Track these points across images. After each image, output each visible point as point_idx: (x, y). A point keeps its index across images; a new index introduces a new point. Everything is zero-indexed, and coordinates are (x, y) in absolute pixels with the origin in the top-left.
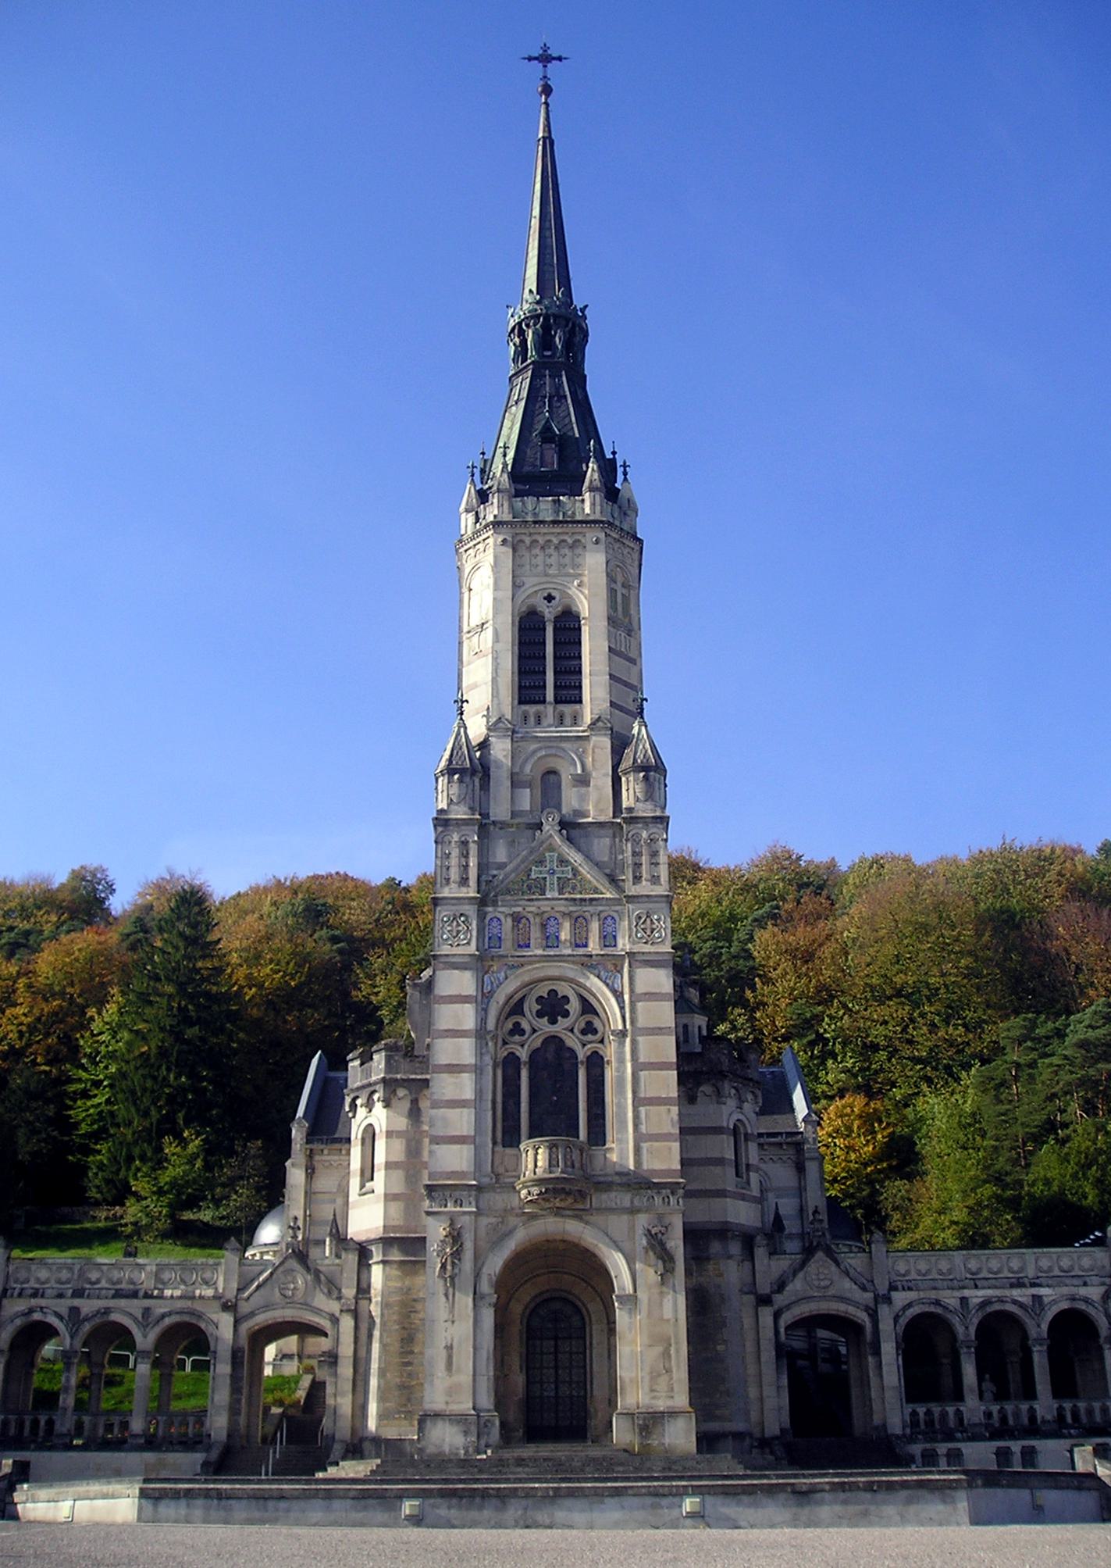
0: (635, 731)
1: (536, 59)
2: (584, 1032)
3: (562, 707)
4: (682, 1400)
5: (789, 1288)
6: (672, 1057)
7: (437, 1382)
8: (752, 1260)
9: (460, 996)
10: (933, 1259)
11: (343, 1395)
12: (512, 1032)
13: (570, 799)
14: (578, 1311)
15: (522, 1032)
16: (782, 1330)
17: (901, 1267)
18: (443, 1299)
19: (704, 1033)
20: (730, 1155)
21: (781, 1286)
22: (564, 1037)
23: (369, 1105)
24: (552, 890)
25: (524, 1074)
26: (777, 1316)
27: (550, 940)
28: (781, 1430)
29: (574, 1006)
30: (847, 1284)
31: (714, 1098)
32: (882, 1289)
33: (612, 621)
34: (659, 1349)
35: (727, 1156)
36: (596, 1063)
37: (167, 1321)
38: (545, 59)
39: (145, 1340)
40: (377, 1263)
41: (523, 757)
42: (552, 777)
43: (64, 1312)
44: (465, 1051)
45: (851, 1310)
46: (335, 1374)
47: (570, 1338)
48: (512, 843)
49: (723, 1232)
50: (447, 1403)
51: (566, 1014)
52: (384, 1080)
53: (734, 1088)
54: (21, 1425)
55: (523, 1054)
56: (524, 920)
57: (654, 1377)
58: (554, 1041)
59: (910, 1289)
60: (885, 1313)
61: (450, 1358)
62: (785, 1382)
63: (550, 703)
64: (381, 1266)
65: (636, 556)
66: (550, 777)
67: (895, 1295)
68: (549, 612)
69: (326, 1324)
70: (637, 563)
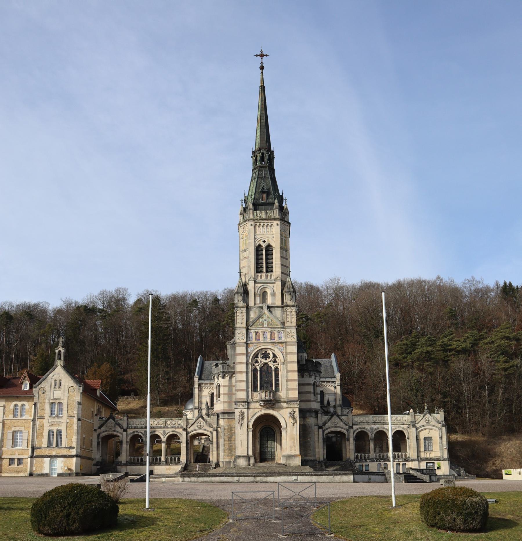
0: (288, 279)
1: (259, 55)
2: (274, 362)
3: (268, 273)
4: (298, 452)
6: (296, 369)
9: (242, 353)
12: (255, 363)
13: (270, 301)
14: (273, 430)
15: (258, 362)
17: (356, 419)
18: (240, 429)
19: (306, 359)
22: (269, 364)
23: (218, 378)
24: (266, 325)
29: (271, 356)
33: (282, 248)
34: (293, 441)
35: (311, 391)
36: (277, 369)
37: (169, 434)
39: (164, 439)
40: (222, 419)
41: (258, 288)
42: (265, 293)
43: (143, 432)
44: (243, 368)
46: (212, 446)
47: (271, 437)
48: (255, 313)
49: (310, 411)
50: (241, 454)
51: (269, 358)
52: (222, 372)
54: (134, 459)
55: (258, 368)
56: (258, 333)
57: (291, 447)
58: (266, 364)
59: (358, 425)
61: (242, 443)
65: (288, 228)
66: (265, 293)
68: (264, 245)
69: (209, 433)
70: (289, 230)
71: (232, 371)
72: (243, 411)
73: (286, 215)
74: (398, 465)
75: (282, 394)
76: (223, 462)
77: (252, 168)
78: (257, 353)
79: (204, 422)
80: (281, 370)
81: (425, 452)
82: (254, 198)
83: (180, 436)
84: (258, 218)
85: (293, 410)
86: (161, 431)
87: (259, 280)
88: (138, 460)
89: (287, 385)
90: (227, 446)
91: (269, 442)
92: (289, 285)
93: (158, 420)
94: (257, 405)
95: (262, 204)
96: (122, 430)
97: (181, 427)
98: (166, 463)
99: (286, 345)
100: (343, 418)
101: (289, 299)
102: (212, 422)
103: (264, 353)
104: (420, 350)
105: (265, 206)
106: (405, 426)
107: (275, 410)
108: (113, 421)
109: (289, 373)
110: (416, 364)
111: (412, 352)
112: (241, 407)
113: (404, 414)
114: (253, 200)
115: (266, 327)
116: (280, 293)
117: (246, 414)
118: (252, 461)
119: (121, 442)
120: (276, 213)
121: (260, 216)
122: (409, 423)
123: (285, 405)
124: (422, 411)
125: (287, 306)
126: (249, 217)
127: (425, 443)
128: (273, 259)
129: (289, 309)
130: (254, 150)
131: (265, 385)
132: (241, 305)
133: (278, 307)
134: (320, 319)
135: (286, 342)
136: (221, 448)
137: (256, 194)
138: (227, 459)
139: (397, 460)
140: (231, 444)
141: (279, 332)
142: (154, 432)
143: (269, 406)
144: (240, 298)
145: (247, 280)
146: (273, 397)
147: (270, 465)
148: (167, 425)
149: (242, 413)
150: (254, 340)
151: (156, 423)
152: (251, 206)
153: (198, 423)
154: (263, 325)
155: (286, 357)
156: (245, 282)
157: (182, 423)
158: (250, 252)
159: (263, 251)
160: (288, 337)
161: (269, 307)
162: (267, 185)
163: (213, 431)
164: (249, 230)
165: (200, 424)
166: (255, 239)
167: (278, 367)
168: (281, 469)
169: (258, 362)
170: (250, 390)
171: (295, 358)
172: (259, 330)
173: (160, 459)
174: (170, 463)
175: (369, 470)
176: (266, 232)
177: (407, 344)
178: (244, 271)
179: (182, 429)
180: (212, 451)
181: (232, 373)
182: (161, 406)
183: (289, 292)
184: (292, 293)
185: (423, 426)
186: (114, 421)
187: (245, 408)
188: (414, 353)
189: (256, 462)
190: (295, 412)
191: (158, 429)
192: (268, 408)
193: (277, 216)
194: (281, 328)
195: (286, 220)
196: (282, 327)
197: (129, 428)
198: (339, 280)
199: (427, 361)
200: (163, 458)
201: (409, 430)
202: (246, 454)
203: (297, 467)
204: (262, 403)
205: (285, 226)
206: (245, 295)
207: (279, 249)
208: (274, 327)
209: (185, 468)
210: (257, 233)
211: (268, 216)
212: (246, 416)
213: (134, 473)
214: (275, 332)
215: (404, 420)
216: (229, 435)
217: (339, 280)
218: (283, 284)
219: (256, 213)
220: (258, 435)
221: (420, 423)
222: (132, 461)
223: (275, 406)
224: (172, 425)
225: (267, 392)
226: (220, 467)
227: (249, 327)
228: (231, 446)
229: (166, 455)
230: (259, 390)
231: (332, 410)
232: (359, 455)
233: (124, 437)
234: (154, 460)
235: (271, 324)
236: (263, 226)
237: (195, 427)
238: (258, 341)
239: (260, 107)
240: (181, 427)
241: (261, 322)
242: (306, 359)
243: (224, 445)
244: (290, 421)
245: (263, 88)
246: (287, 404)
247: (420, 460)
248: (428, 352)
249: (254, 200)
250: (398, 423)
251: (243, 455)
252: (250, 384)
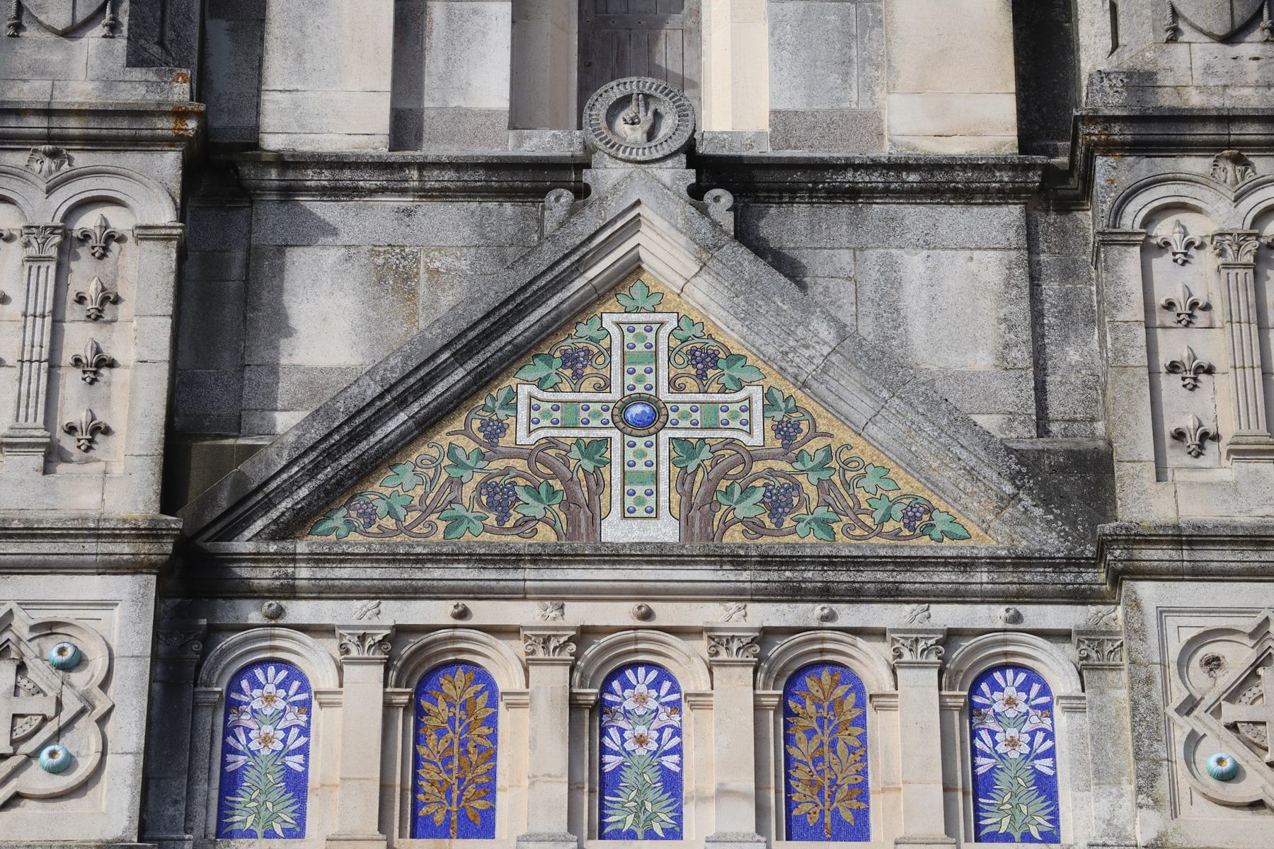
56: (454, 686)
160: (1208, 759)
196: (1053, 543)
227: (243, 545)
235: (778, 503)
241: (533, 455)
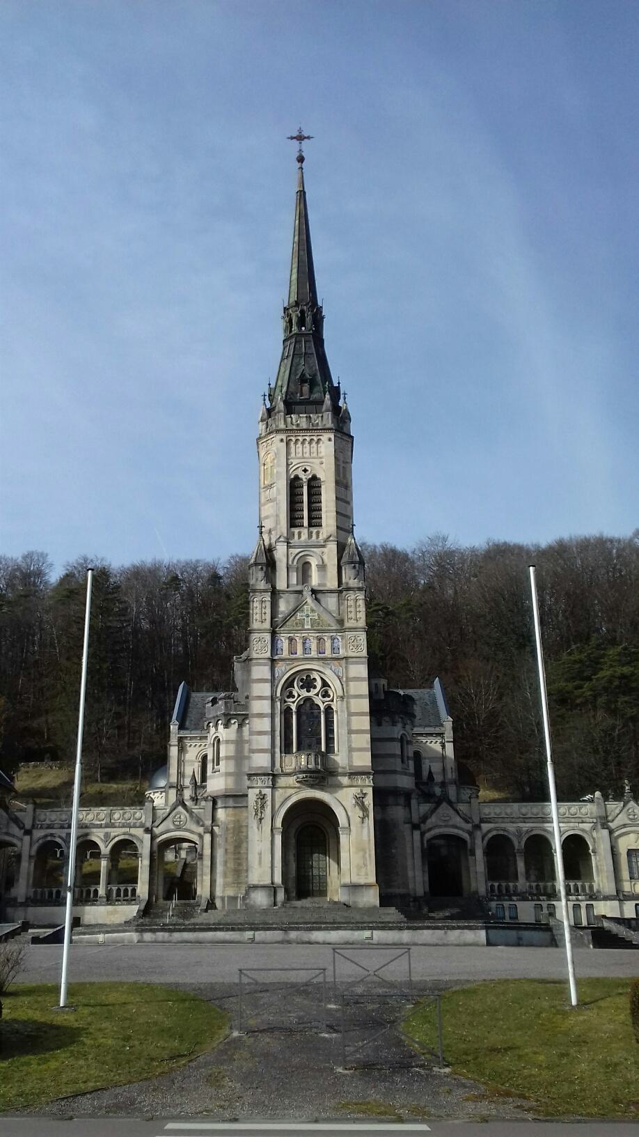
1: (295, 138)
2: (323, 696)
3: (311, 529)
4: (372, 879)
5: (429, 821)
6: (367, 709)
7: (254, 870)
8: (410, 806)
10: (503, 807)
11: (206, 875)
12: (288, 697)
13: (315, 580)
15: (294, 697)
16: (425, 842)
18: (257, 830)
20: (398, 752)
21: (424, 819)
22: (314, 699)
23: (216, 726)
25: (294, 717)
26: (422, 835)
27: (307, 650)
28: (425, 893)
29: (319, 684)
30: (458, 819)
31: (391, 723)
32: (477, 821)
33: (337, 483)
34: (361, 854)
36: (329, 710)
37: (117, 839)
38: (300, 138)
39: (105, 849)
40: (222, 808)
42: (307, 565)
45: (460, 833)
46: (202, 865)
48: (288, 602)
51: (315, 687)
52: (224, 715)
53: (401, 718)
54: (43, 893)
55: (294, 707)
56: (294, 641)
57: (359, 868)
58: (308, 699)
60: (478, 834)
61: (260, 858)
62: (427, 869)
63: (306, 528)
64: (224, 810)
65: (350, 445)
66: (306, 565)
67: (483, 825)
68: (304, 477)
69: (195, 838)
70: (350, 449)
71: (243, 713)
72: (263, 793)
73: (345, 422)
74: (576, 907)
75: (340, 758)
76: (223, 898)
77: (283, 338)
78: (291, 679)
79: (187, 815)
80: (337, 712)
81: (631, 882)
82: (287, 392)
83: (138, 844)
84: (294, 427)
85: (362, 791)
86: (99, 834)
87: (295, 540)
88: (51, 894)
89: (349, 741)
90: (231, 865)
91: (315, 855)
92: (351, 550)
93: (96, 810)
94: (292, 781)
95: (301, 403)
96: (23, 831)
97: (142, 826)
98: (108, 900)
99: (347, 663)
100: (462, 807)
101: (352, 577)
102: (202, 814)
103: (305, 678)
104: (608, 673)
105: (307, 407)
106: (587, 826)
107: (326, 792)
108: (7, 816)
109: (353, 718)
110: (601, 700)
111: (593, 677)
112: (260, 784)
113: (584, 801)
114: (284, 396)
115: (308, 630)
116: (335, 565)
117: (269, 798)
118: (281, 896)
119: (18, 857)
120: (327, 419)
121: (298, 425)
122: (595, 821)
123: (345, 780)
124: (619, 796)
125: (348, 589)
126: (277, 426)
127: (630, 862)
128: (321, 502)
129: (352, 595)
130: (286, 305)
131: (306, 741)
132: (262, 588)
133: (331, 591)
134: (411, 614)
135: (346, 658)
136: (219, 868)
137: (290, 384)
138: (230, 892)
139: (574, 898)
140: (238, 859)
141: (333, 639)
142: (87, 835)
143: (314, 783)
144: (261, 575)
145: (273, 541)
146: (323, 764)
147: (317, 906)
148: (112, 821)
149: (262, 797)
150: (285, 654)
151: (90, 817)
152: (281, 406)
153: (174, 817)
154: (303, 626)
155: (347, 686)
156: (270, 545)
157: (144, 817)
158: (278, 489)
159: (302, 487)
160: (351, 648)
161: (314, 592)
162: (311, 368)
163: (205, 833)
164: (278, 449)
165: (178, 820)
166: (288, 465)
167: (332, 706)
168: (340, 913)
169: (294, 697)
170: (278, 750)
171: (363, 688)
172: (296, 635)
173: (96, 892)
174: (117, 900)
175: (517, 918)
176: (308, 455)
177: (581, 661)
178: (268, 524)
179: (142, 830)
180: (202, 875)
181: (243, 717)
182: (102, 782)
183: (352, 563)
184: (357, 565)
185: (625, 826)
186: (7, 813)
187: (267, 787)
188: (598, 679)
189: (288, 898)
190: (365, 794)
191: (94, 830)
192: (312, 786)
193: (330, 425)
194: (337, 631)
195: (345, 430)
196: (338, 628)
197: (37, 828)
198: (445, 539)
199: (624, 694)
200: (102, 891)
201: (595, 834)
202: (268, 882)
203: (370, 910)
204: (301, 776)
205: (344, 443)
206: (269, 569)
207: (332, 485)
208: (324, 628)
209: (146, 911)
210: (293, 455)
211: (313, 424)
212: (269, 803)
213: (41, 923)
214: (325, 638)
215: (562, 813)
216: (236, 841)
217: (445, 539)
218: (341, 548)
219: (290, 419)
220: (293, 841)
221: (617, 819)
222: (39, 897)
223: (326, 784)
224: (123, 821)
225: (310, 754)
226: (216, 908)
227: (277, 630)
228: (239, 864)
229: (109, 883)
230: (294, 750)
231: (438, 791)
232: (496, 884)
233: (26, 847)
234: (84, 894)
236: (303, 443)
237: (168, 824)
238: (294, 656)
239: (297, 228)
240: (142, 826)
242: (386, 690)
243: (225, 862)
244: (356, 814)
245: (302, 194)
246: (349, 778)
247: (621, 898)
248: (623, 677)
249: (286, 396)
250: (573, 820)
251: (262, 883)
252: (279, 738)
